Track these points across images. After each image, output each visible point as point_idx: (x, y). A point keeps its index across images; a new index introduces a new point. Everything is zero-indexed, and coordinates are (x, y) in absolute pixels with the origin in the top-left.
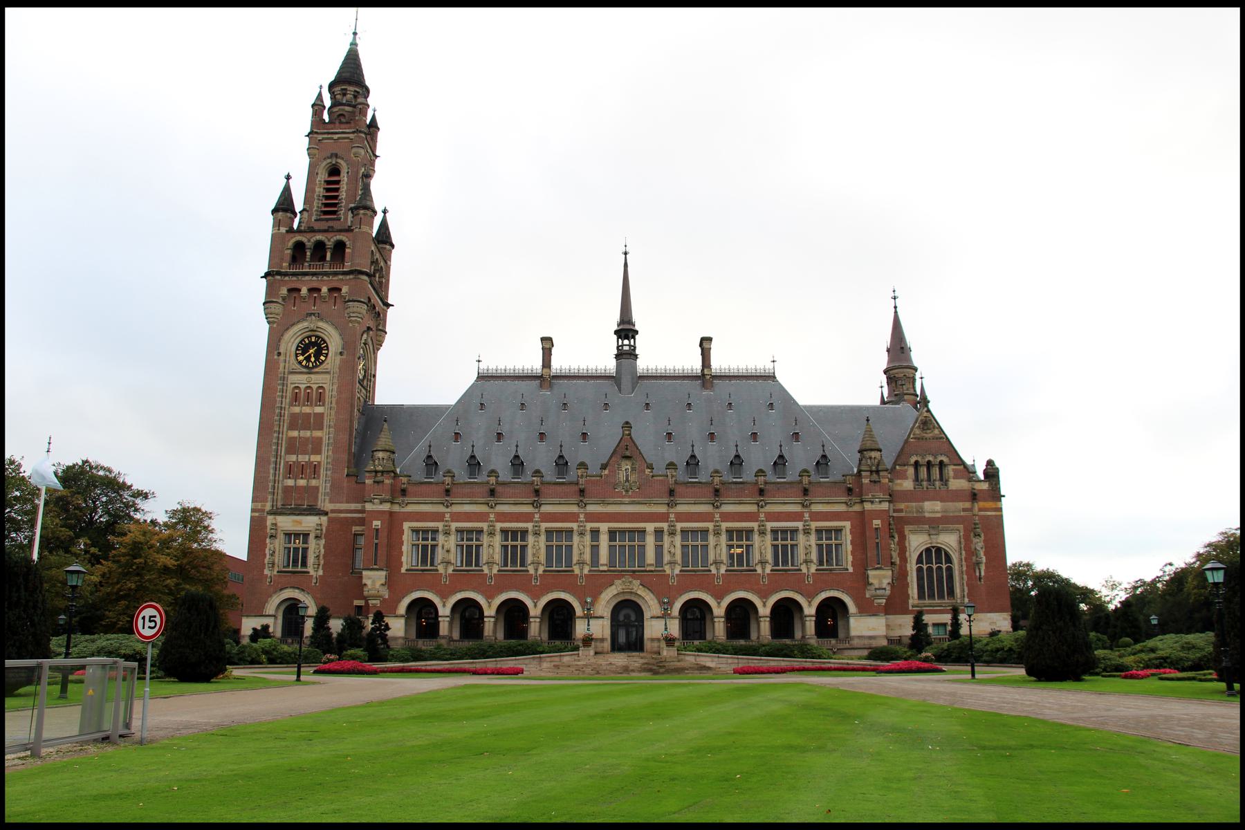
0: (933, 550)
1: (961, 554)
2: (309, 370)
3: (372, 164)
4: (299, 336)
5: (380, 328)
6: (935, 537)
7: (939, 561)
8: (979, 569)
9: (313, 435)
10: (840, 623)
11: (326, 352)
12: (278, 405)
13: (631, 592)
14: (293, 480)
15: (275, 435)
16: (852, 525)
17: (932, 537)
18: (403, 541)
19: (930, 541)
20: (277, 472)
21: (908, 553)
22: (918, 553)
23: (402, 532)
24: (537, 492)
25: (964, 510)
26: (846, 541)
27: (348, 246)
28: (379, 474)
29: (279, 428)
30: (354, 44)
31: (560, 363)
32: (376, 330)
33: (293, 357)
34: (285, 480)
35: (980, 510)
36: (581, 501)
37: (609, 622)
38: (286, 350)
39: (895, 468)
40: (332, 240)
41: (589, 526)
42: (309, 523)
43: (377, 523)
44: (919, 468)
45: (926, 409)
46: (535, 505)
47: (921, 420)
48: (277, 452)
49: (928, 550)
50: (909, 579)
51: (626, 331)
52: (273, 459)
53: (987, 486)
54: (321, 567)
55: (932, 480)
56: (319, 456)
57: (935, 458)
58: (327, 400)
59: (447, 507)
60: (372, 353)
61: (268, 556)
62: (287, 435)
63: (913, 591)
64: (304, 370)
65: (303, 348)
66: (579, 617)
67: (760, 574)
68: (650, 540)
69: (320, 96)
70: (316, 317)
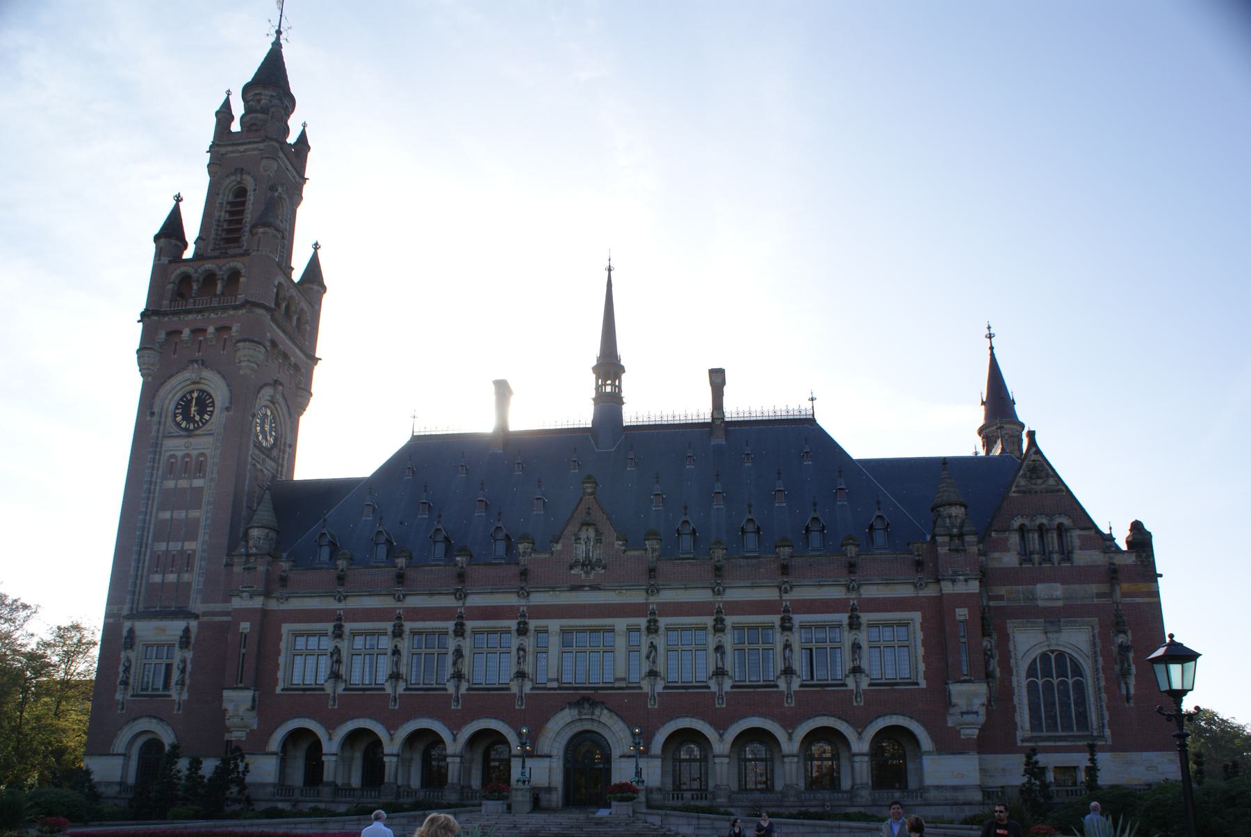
0: (1053, 657)
1: (1096, 661)
2: (189, 433)
4: (178, 391)
5: (302, 386)
6: (1055, 635)
7: (1062, 673)
8: (1127, 684)
9: (190, 516)
10: (911, 766)
11: (211, 409)
12: (146, 479)
13: (592, 719)
14: (161, 576)
15: (140, 517)
16: (924, 618)
17: (1049, 635)
18: (280, 650)
19: (1047, 643)
20: (141, 565)
21: (1012, 661)
22: (1029, 661)
23: (280, 638)
24: (461, 577)
25: (1099, 595)
26: (915, 641)
27: (243, 274)
28: (252, 560)
29: (147, 508)
33: (170, 419)
34: (151, 576)
35: (1124, 595)
36: (522, 588)
37: (561, 763)
38: (162, 409)
39: (990, 536)
40: (224, 268)
41: (533, 624)
43: (245, 626)
44: (1026, 535)
45: (1034, 449)
46: (458, 596)
47: (1027, 466)
48: (142, 539)
49: (1045, 657)
50: (1016, 700)
52: (136, 548)
53: (1134, 559)
54: (186, 688)
55: (1047, 551)
56: (195, 542)
57: (1051, 517)
58: (208, 470)
59: (340, 601)
60: (287, 416)
61: (121, 675)
62: (157, 517)
63: (1023, 717)
64: (184, 433)
65: (184, 406)
66: (515, 756)
67: (784, 692)
68: (620, 643)
70: (198, 365)
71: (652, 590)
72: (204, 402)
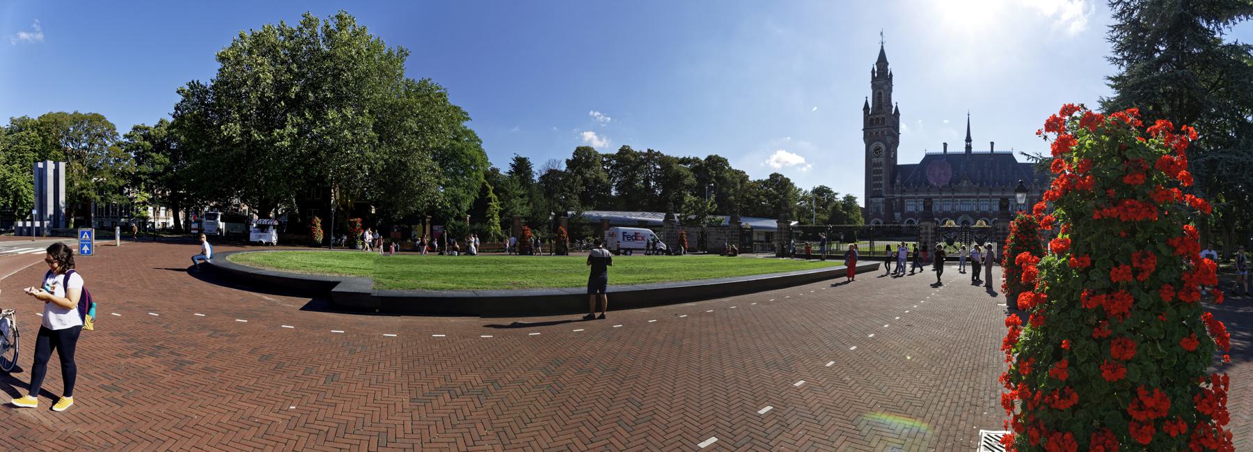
2: (878, 157)
3: (891, 88)
30: (882, 47)
31: (949, 150)
32: (896, 143)
41: (955, 199)
42: (881, 199)
51: (968, 139)
69: (873, 69)
71: (978, 193)
72: (880, 148)
